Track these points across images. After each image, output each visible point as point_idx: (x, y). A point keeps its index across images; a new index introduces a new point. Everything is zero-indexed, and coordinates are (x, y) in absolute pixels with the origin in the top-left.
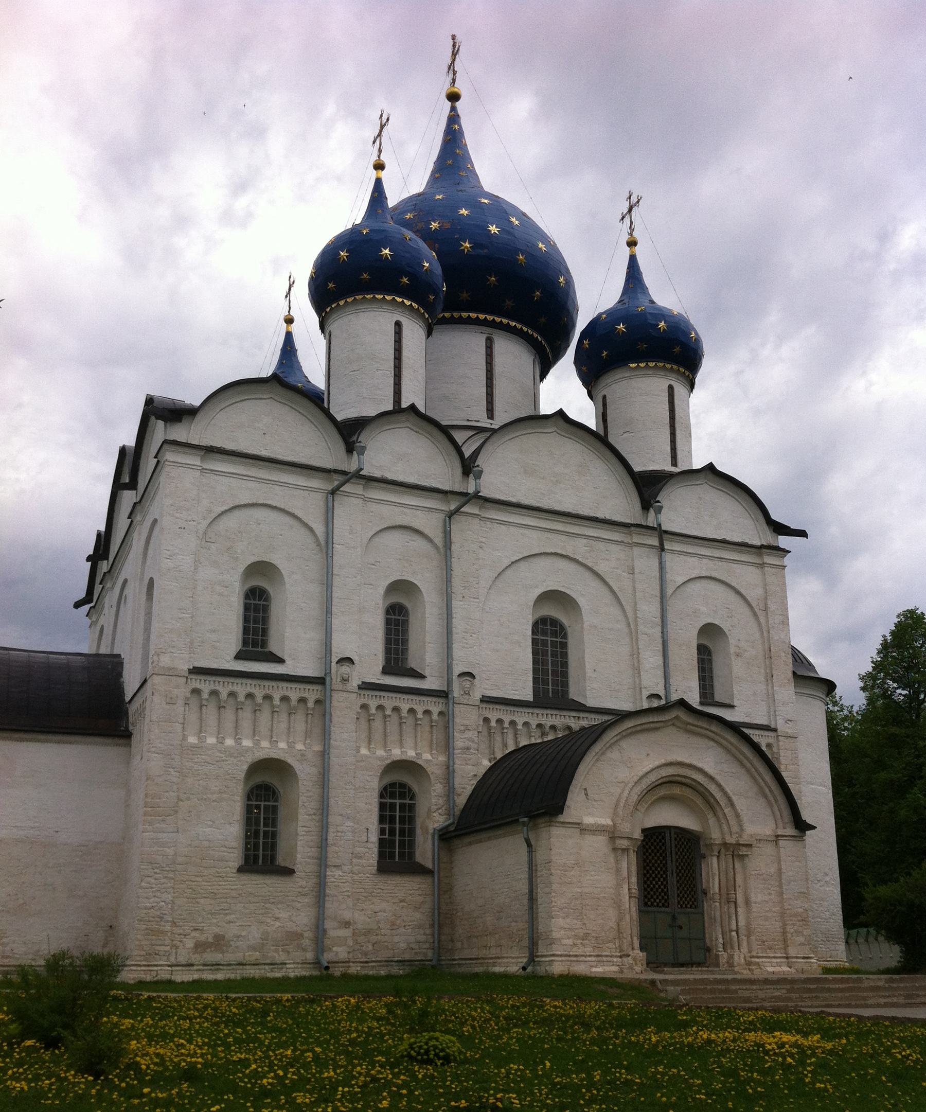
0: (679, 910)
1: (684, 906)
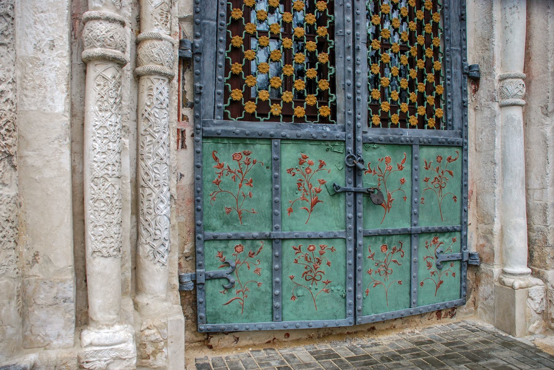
0: (372, 134)
1: (395, 118)
